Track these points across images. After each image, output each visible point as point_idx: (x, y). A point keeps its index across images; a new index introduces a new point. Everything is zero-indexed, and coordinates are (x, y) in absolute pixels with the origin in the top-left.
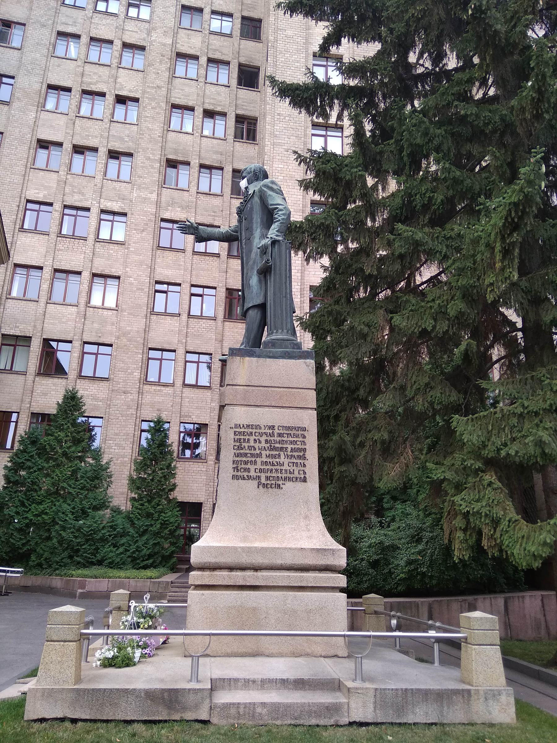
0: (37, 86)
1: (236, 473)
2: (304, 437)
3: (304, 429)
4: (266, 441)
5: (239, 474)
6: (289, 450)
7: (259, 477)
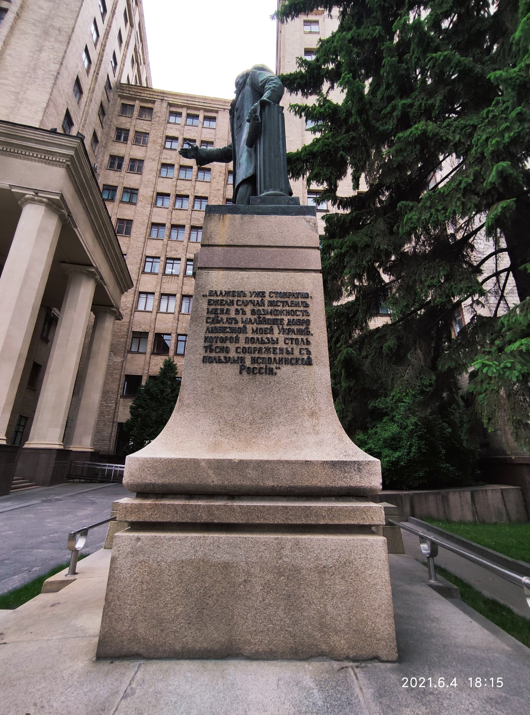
0: (151, 194)
1: (208, 354)
2: (307, 306)
3: (307, 296)
4: (253, 312)
5: (213, 355)
6: (286, 322)
7: (242, 360)
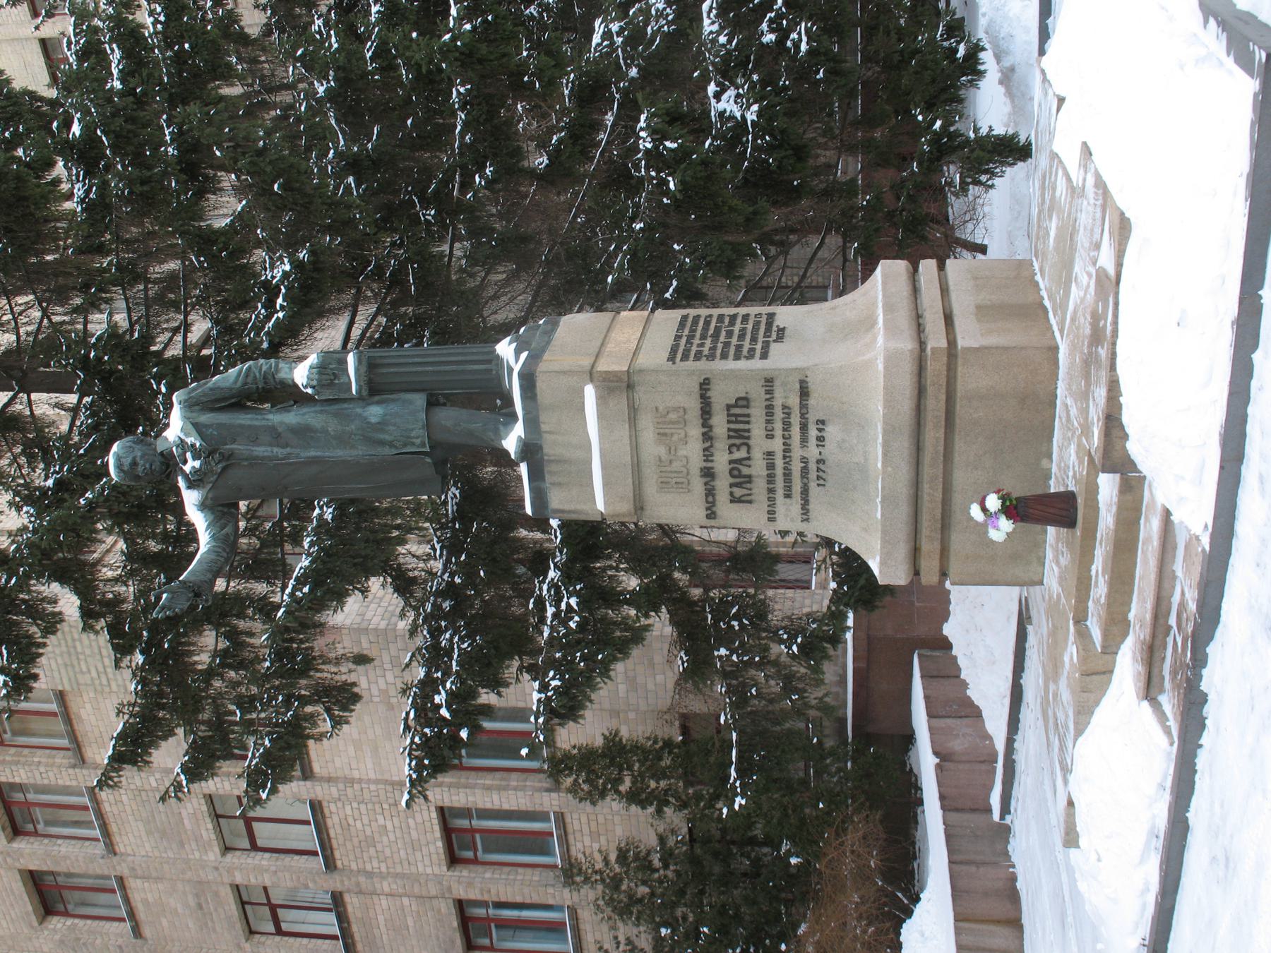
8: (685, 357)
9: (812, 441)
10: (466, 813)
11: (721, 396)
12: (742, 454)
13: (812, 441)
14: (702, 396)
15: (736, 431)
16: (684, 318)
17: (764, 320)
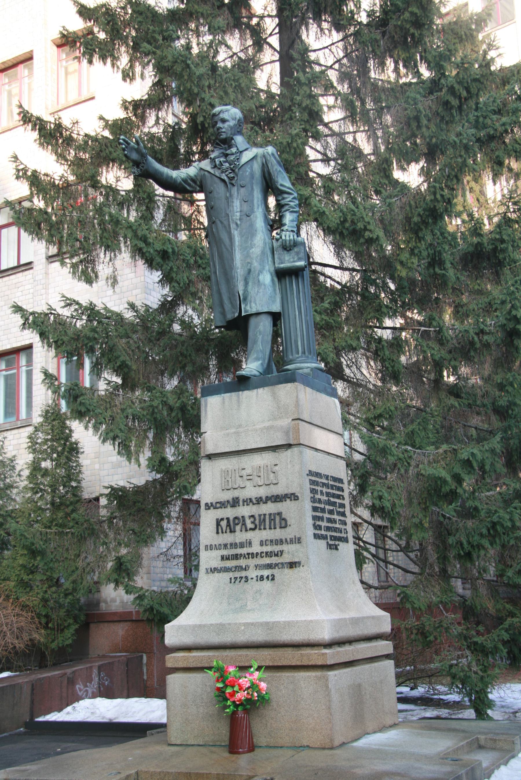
1: (317, 532)
8: (312, 482)
9: (260, 573)
10: (30, 362)
11: (286, 508)
12: (250, 525)
13: (260, 573)
14: (286, 495)
15: (264, 520)
16: (341, 481)
17: (343, 535)
